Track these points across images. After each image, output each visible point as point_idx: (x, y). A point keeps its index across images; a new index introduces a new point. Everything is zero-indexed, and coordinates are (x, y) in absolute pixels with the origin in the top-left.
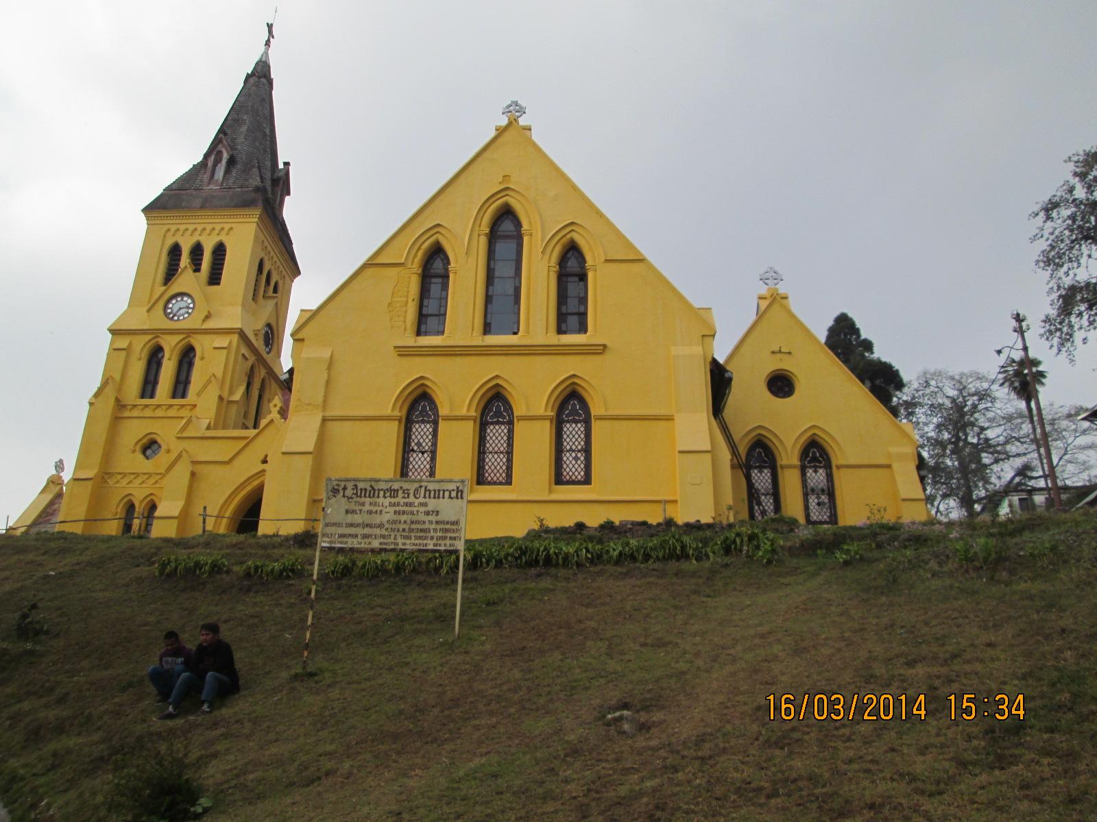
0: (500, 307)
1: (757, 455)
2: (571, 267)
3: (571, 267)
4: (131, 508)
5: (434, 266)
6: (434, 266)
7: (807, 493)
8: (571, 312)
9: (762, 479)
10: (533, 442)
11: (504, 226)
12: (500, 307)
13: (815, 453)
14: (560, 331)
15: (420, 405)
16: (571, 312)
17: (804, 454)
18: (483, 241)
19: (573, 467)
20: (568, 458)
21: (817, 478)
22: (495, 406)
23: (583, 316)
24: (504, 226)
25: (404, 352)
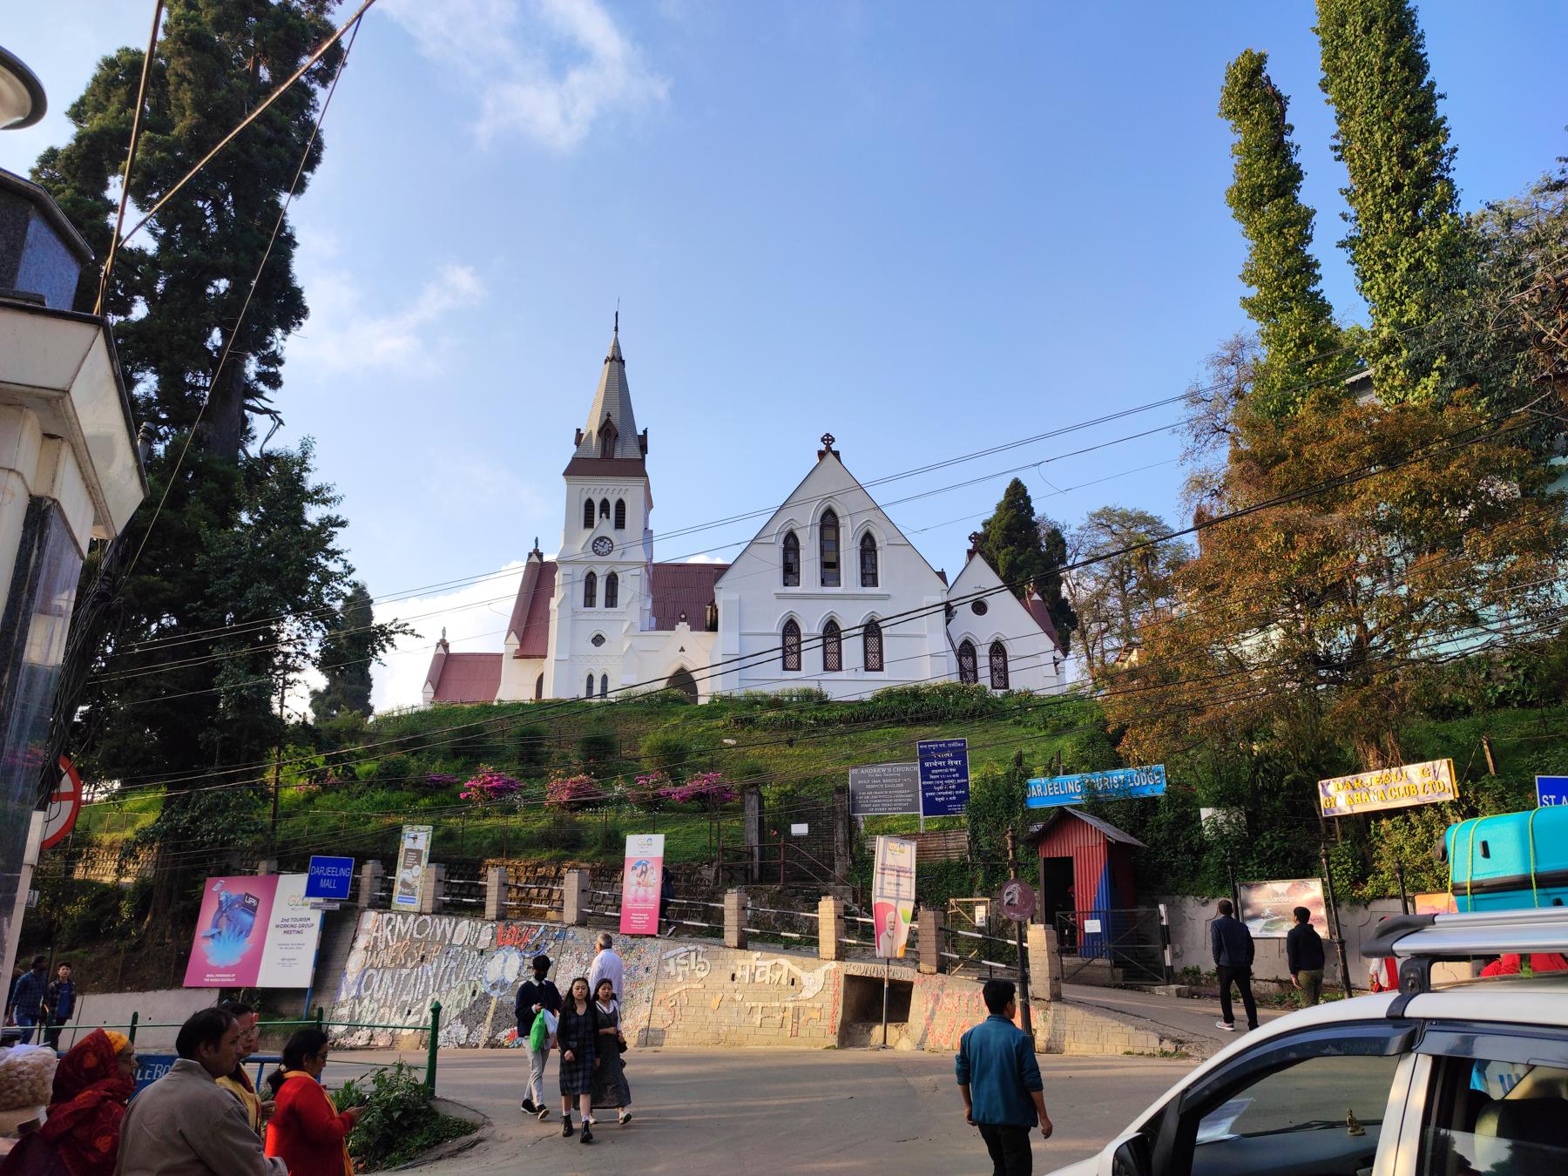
0: (830, 569)
1: (966, 650)
2: (868, 546)
3: (868, 546)
4: (590, 678)
5: (791, 544)
6: (791, 544)
7: (993, 669)
8: (869, 576)
9: (968, 662)
10: (852, 650)
11: (829, 522)
12: (830, 569)
13: (998, 649)
14: (864, 585)
15: (791, 628)
16: (869, 576)
17: (991, 650)
18: (817, 529)
19: (874, 661)
20: (870, 656)
21: (998, 661)
22: (832, 631)
23: (875, 576)
24: (829, 522)
25: (779, 596)
